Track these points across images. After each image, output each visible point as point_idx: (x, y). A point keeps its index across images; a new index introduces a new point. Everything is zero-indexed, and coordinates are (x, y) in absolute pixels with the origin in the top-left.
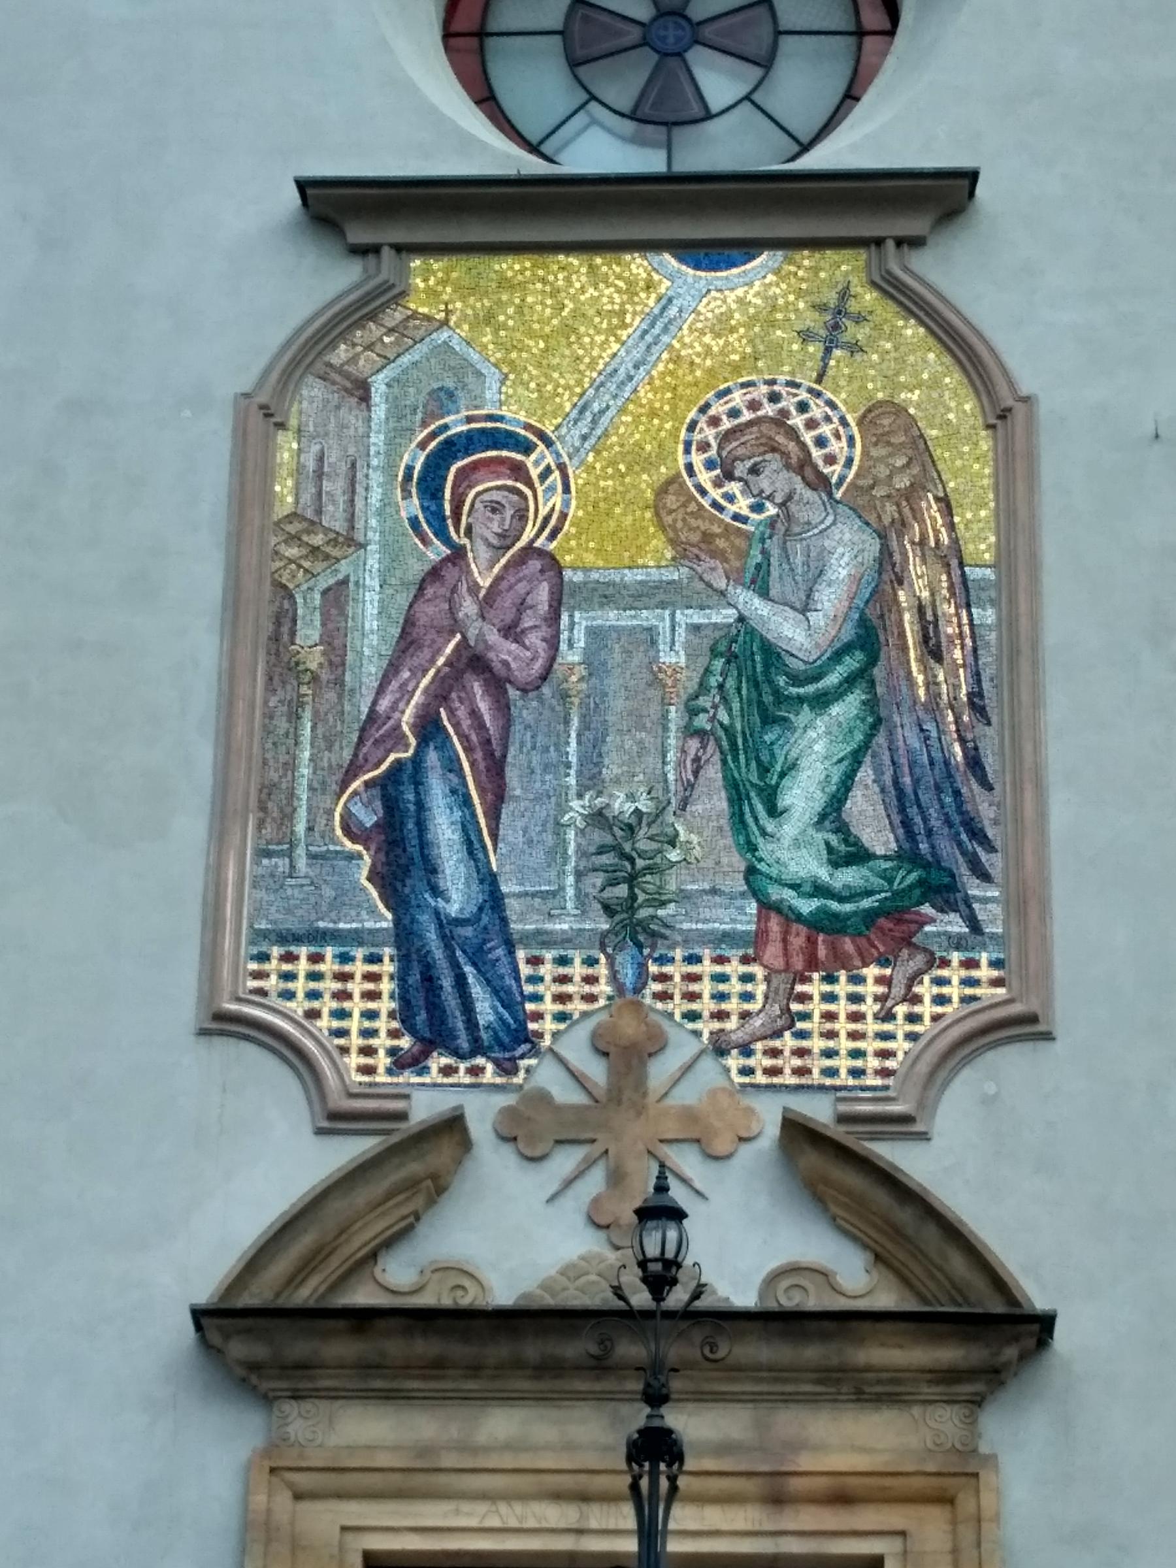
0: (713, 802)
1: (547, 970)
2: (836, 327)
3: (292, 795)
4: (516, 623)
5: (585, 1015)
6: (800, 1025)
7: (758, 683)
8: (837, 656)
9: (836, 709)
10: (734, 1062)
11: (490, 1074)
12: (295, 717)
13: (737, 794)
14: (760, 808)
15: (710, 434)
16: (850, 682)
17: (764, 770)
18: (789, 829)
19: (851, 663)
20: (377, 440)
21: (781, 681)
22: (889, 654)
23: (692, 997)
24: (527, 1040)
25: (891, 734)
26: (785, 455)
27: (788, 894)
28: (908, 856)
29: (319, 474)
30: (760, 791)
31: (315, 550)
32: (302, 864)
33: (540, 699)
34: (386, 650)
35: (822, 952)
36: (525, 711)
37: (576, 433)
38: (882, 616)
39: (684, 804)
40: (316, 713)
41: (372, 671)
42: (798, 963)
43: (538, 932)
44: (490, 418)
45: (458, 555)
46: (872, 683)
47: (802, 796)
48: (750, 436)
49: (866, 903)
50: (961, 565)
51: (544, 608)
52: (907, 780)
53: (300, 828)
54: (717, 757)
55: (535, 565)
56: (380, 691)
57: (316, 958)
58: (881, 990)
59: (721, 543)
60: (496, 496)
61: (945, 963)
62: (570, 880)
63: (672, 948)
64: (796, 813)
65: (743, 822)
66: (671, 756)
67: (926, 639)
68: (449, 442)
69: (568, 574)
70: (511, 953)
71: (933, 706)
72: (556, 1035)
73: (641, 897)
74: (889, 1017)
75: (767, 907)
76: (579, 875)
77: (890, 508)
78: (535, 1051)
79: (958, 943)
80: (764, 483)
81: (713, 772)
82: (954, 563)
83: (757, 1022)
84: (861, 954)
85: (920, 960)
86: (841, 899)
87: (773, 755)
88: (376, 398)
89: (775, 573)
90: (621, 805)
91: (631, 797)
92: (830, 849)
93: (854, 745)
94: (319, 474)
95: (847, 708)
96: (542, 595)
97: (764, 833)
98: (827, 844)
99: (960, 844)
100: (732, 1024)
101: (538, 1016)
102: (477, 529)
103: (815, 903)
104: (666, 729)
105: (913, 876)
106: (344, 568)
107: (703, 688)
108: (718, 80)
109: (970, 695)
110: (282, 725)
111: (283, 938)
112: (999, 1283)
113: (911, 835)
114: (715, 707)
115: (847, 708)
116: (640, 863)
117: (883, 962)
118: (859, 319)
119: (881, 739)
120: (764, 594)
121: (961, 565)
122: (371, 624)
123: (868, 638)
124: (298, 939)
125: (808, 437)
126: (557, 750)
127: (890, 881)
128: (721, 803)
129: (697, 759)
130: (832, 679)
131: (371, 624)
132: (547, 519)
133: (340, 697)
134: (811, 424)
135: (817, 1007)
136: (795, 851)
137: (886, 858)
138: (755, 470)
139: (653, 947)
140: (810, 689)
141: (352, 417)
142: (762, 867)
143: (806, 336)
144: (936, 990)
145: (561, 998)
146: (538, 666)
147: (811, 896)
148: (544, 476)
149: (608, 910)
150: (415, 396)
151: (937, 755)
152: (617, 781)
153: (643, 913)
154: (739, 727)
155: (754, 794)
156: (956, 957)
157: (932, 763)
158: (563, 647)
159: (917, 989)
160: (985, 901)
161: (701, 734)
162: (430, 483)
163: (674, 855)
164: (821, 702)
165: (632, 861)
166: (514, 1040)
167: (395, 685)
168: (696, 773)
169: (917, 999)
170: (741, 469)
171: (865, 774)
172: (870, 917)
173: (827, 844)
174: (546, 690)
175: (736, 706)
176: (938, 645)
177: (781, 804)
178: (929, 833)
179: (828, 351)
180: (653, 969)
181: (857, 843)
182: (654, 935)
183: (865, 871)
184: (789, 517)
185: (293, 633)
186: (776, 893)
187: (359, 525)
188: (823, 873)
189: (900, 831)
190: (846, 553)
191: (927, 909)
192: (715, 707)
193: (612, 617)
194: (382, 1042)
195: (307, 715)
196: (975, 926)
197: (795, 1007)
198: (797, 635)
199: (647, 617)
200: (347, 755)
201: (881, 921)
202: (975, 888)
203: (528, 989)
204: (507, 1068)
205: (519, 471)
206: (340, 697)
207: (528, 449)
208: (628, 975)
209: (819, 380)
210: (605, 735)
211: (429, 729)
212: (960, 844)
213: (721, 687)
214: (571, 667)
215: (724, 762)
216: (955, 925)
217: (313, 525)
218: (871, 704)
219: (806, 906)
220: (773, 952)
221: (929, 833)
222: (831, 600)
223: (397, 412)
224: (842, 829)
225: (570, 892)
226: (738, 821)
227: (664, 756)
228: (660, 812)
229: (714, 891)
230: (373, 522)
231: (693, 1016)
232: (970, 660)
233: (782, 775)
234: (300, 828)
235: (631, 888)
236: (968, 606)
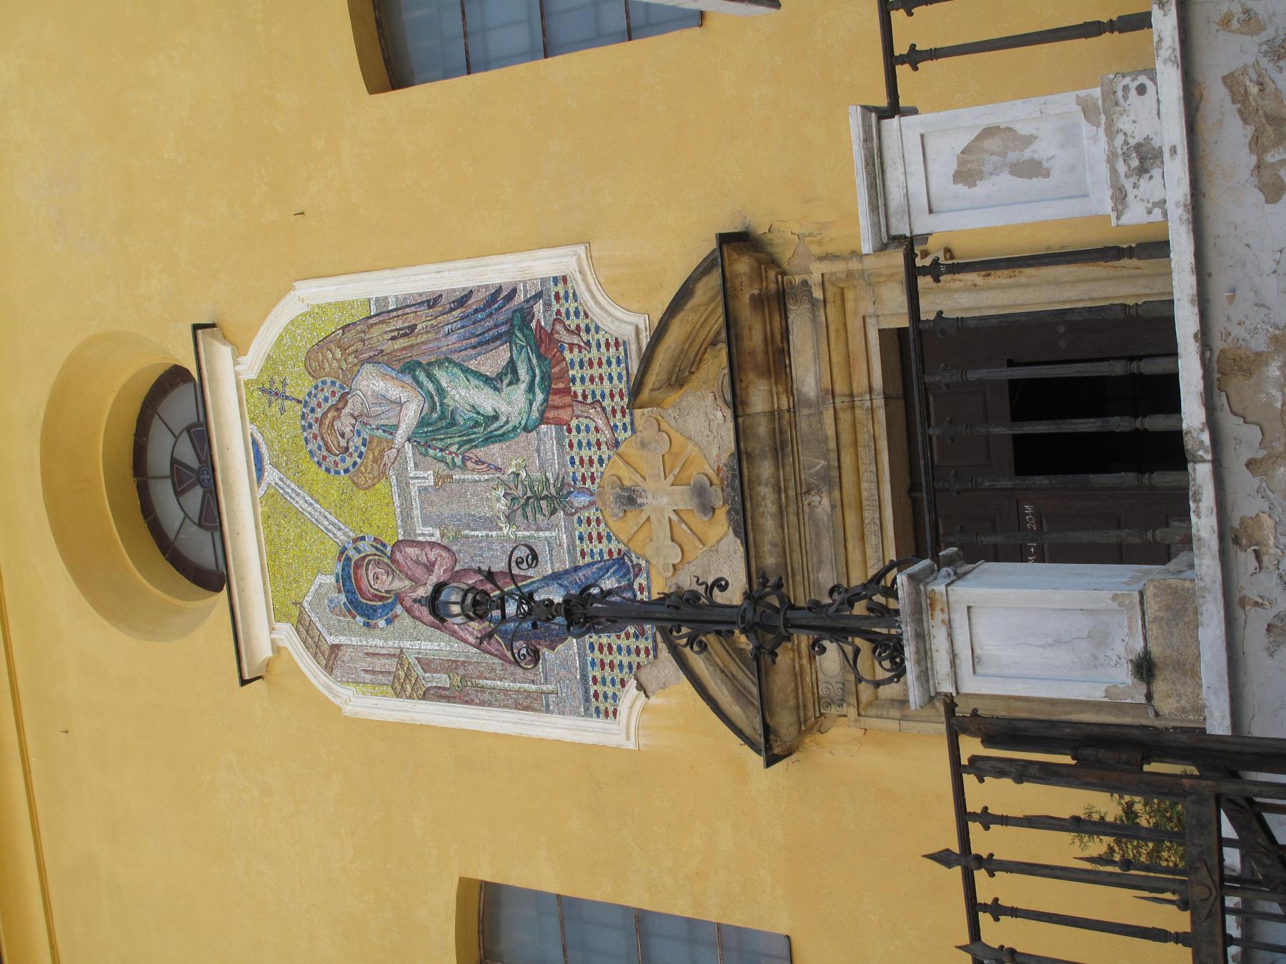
0: (494, 452)
1: (586, 546)
2: (276, 394)
3: (518, 691)
4: (425, 565)
5: (606, 525)
6: (598, 397)
7: (439, 426)
8: (420, 385)
9: (444, 384)
10: (621, 436)
11: (641, 580)
12: (483, 689)
13: (489, 439)
14: (495, 425)
15: (331, 459)
16: (430, 377)
17: (477, 424)
18: (504, 408)
19: (422, 377)
20: (355, 641)
21: (435, 415)
22: (415, 355)
23: (591, 462)
24: (623, 558)
25: (452, 352)
26: (334, 418)
27: (535, 408)
28: (508, 337)
29: (373, 672)
30: (487, 426)
31: (406, 676)
32: (550, 687)
33: (460, 551)
34: (446, 637)
35: (561, 385)
36: (464, 561)
37: (339, 534)
38: (399, 361)
39: (497, 469)
40: (479, 677)
41: (457, 645)
42: (568, 399)
43: (569, 552)
44: (337, 581)
45: (399, 598)
46: (430, 364)
47: (487, 401)
48: (328, 439)
49: (534, 361)
50: (370, 317)
51: (417, 551)
52: (474, 341)
53: (533, 687)
54: (474, 451)
55: (398, 556)
56: (466, 641)
57: (595, 680)
58: (576, 350)
59: (377, 452)
60: (371, 577)
61: (558, 313)
62: (541, 534)
63: (567, 473)
64: (496, 405)
65: (502, 435)
66: (476, 477)
67: (405, 335)
68: (351, 602)
69: (401, 538)
70: (580, 568)
71: (436, 328)
72: (619, 541)
73: (545, 492)
74: (588, 343)
75: (543, 419)
76: (539, 529)
77: (351, 359)
78: (627, 553)
79: (548, 305)
80: (348, 430)
81: (481, 453)
82: (371, 321)
83: (601, 423)
84: (558, 363)
85: (558, 327)
86: (534, 376)
87: (470, 419)
88: (337, 642)
89: (386, 422)
90: (502, 505)
91: (498, 500)
92: (510, 384)
93: (460, 373)
94: (373, 672)
96: (409, 550)
97: (507, 422)
98: (508, 385)
99: (500, 308)
100: (603, 439)
101: (610, 552)
102: (387, 588)
103: (537, 390)
104: (464, 481)
105: (518, 334)
106: (412, 660)
107: (442, 460)
109: (430, 307)
110: (486, 696)
111: (587, 700)
113: (498, 337)
114: (451, 453)
116: (529, 494)
117: (561, 350)
118: (272, 382)
119: (455, 357)
120: (397, 426)
121: (370, 317)
122: (435, 646)
123: (410, 368)
124: (587, 691)
125: (326, 406)
126: (480, 542)
127: (522, 347)
128: (495, 448)
129: (476, 463)
130: (431, 387)
131: (435, 646)
132: (377, 549)
133: (470, 663)
134: (319, 405)
135: (589, 387)
136: (512, 404)
137: (511, 350)
138: (343, 436)
139: (569, 485)
140: (436, 399)
141: (346, 655)
142: (523, 423)
143: (283, 410)
144: (572, 317)
145: (600, 538)
146: (444, 554)
147: (534, 394)
148: (359, 551)
149: (553, 512)
150: (333, 620)
151: (459, 324)
152: (491, 508)
153: (553, 491)
154: (457, 439)
155: (488, 430)
156: (555, 307)
157: (463, 327)
158: (433, 539)
159: (573, 327)
160: (526, 291)
161: (464, 460)
162: (369, 614)
163: (524, 475)
164: (441, 391)
165: (529, 498)
167: (461, 633)
168: (483, 463)
169: (578, 327)
170: (343, 443)
171: (472, 365)
172: (539, 357)
173: (508, 385)
174: (454, 548)
175: (449, 441)
176: (408, 327)
177: (492, 413)
178: (496, 326)
179: (287, 398)
180: (580, 484)
181: (506, 367)
182: (562, 485)
183: (519, 364)
184: (361, 415)
185: (445, 689)
186: (535, 415)
187: (392, 651)
188: (523, 386)
189: (498, 343)
190: (374, 384)
191: (533, 325)
192: (451, 453)
193: (417, 512)
194: (632, 643)
195: (481, 682)
196: (539, 295)
197: (589, 400)
199: (414, 492)
200: (496, 660)
201: (542, 350)
202: (520, 298)
203: (597, 557)
204: (638, 570)
205: (358, 566)
206: (470, 663)
207: (349, 559)
208: (581, 500)
209: (299, 402)
210: (469, 515)
212: (500, 308)
213: (441, 450)
214: (443, 535)
215: (476, 447)
216: (539, 307)
217: (396, 677)
218: (439, 363)
219: (540, 397)
220: (564, 414)
221: (496, 326)
222: (394, 389)
223: (341, 632)
224: (500, 377)
225: (547, 534)
226: (502, 437)
227: (476, 481)
228: (503, 483)
229: (538, 451)
230: (390, 643)
231: (601, 461)
232: (413, 309)
233: (478, 413)
234: (533, 687)
235: (542, 499)
236: (390, 312)
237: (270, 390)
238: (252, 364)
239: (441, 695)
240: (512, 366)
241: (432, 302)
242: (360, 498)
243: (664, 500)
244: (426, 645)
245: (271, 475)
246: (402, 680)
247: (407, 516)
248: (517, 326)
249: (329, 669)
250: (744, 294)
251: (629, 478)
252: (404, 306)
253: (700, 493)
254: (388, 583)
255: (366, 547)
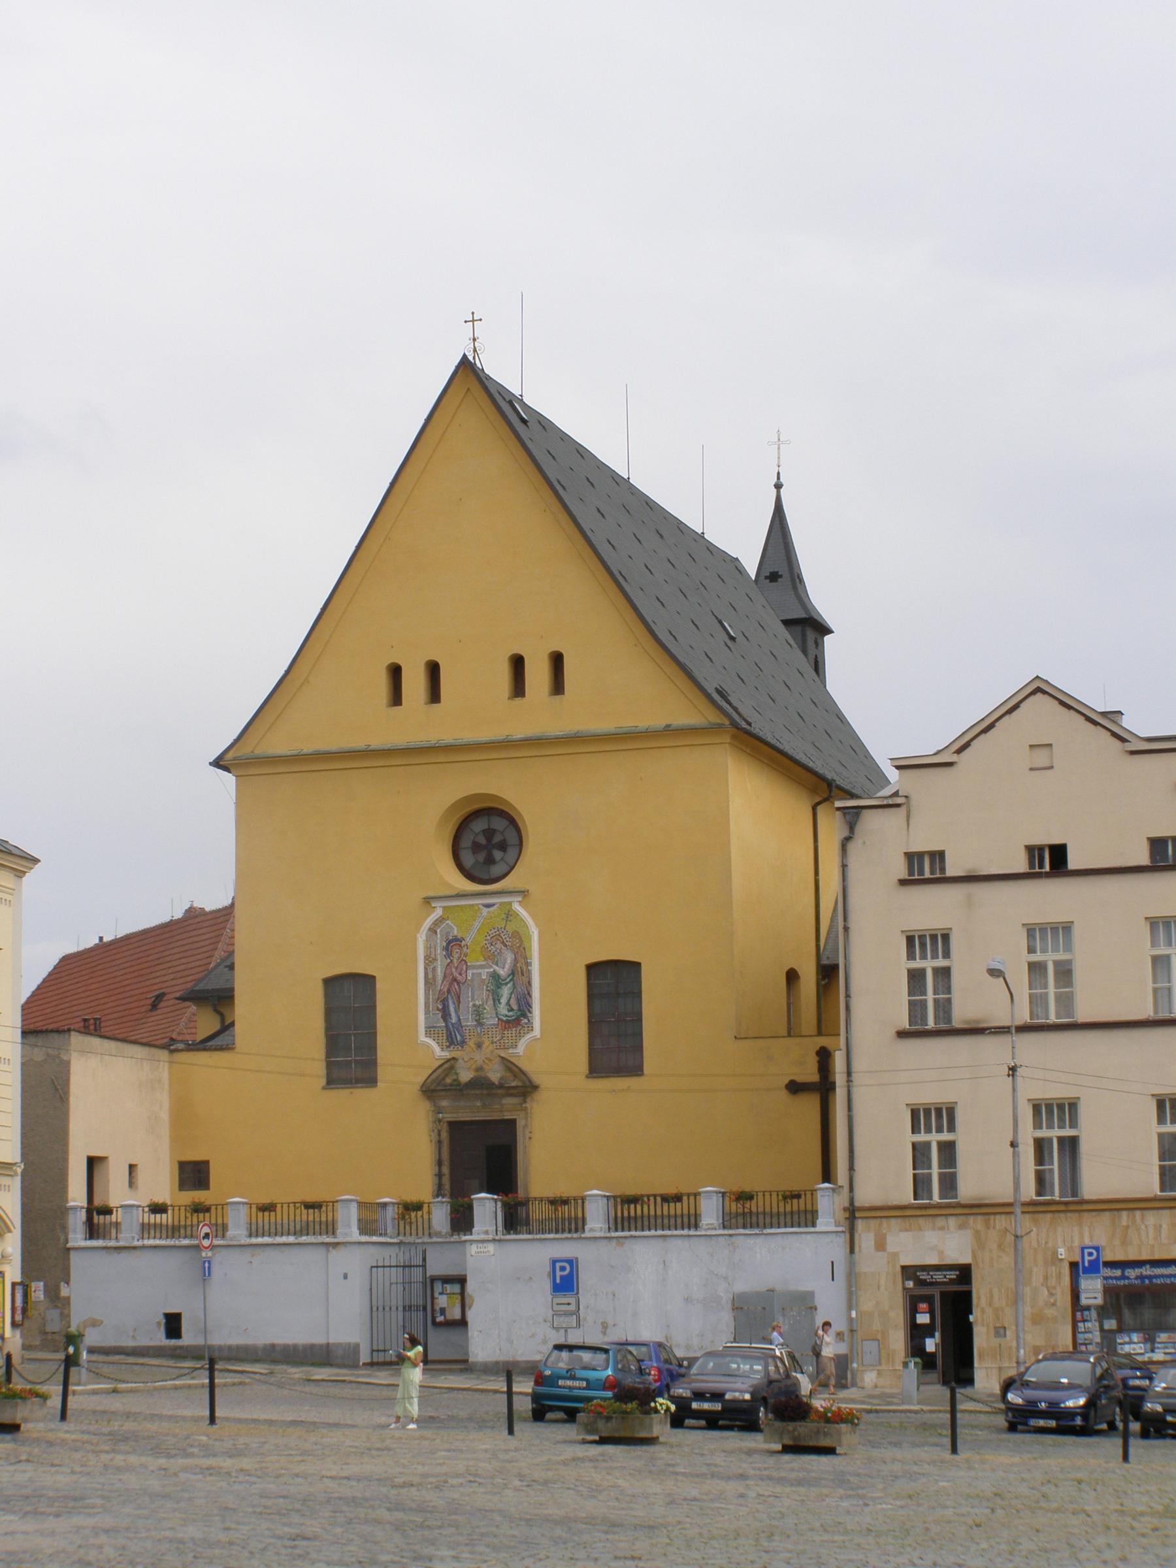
28: (519, 1010)
47: (504, 1000)
95: (510, 985)
108: (498, 855)
112: (530, 1081)
115: (510, 985)
123: (513, 973)
136: (503, 1009)
155: (496, 1000)
162: (446, 948)
166: (463, 1043)
190: (509, 958)
198: (502, 972)
211: (449, 991)
222: (507, 966)
237: (509, 915)
238: (517, 907)
239: (426, 974)
240: (511, 1010)
241: (530, 983)
242: (478, 949)
243: (479, 1057)
244: (439, 970)
245: (485, 910)
246: (429, 960)
247: (474, 967)
248: (520, 1017)
249: (430, 929)
250: (524, 1088)
251: (484, 1046)
252: (529, 972)
253: (479, 1069)
254: (456, 956)
255: (465, 949)
